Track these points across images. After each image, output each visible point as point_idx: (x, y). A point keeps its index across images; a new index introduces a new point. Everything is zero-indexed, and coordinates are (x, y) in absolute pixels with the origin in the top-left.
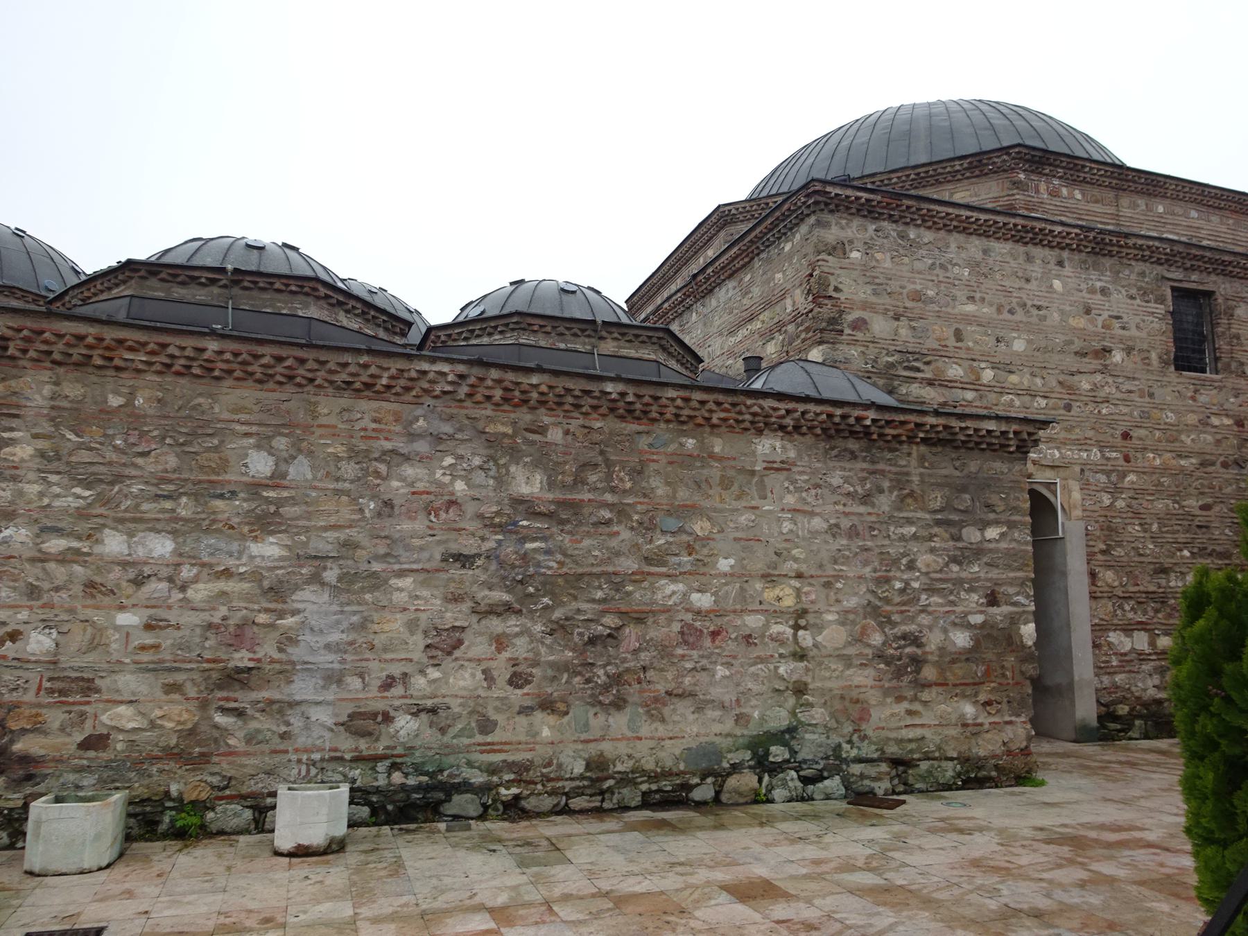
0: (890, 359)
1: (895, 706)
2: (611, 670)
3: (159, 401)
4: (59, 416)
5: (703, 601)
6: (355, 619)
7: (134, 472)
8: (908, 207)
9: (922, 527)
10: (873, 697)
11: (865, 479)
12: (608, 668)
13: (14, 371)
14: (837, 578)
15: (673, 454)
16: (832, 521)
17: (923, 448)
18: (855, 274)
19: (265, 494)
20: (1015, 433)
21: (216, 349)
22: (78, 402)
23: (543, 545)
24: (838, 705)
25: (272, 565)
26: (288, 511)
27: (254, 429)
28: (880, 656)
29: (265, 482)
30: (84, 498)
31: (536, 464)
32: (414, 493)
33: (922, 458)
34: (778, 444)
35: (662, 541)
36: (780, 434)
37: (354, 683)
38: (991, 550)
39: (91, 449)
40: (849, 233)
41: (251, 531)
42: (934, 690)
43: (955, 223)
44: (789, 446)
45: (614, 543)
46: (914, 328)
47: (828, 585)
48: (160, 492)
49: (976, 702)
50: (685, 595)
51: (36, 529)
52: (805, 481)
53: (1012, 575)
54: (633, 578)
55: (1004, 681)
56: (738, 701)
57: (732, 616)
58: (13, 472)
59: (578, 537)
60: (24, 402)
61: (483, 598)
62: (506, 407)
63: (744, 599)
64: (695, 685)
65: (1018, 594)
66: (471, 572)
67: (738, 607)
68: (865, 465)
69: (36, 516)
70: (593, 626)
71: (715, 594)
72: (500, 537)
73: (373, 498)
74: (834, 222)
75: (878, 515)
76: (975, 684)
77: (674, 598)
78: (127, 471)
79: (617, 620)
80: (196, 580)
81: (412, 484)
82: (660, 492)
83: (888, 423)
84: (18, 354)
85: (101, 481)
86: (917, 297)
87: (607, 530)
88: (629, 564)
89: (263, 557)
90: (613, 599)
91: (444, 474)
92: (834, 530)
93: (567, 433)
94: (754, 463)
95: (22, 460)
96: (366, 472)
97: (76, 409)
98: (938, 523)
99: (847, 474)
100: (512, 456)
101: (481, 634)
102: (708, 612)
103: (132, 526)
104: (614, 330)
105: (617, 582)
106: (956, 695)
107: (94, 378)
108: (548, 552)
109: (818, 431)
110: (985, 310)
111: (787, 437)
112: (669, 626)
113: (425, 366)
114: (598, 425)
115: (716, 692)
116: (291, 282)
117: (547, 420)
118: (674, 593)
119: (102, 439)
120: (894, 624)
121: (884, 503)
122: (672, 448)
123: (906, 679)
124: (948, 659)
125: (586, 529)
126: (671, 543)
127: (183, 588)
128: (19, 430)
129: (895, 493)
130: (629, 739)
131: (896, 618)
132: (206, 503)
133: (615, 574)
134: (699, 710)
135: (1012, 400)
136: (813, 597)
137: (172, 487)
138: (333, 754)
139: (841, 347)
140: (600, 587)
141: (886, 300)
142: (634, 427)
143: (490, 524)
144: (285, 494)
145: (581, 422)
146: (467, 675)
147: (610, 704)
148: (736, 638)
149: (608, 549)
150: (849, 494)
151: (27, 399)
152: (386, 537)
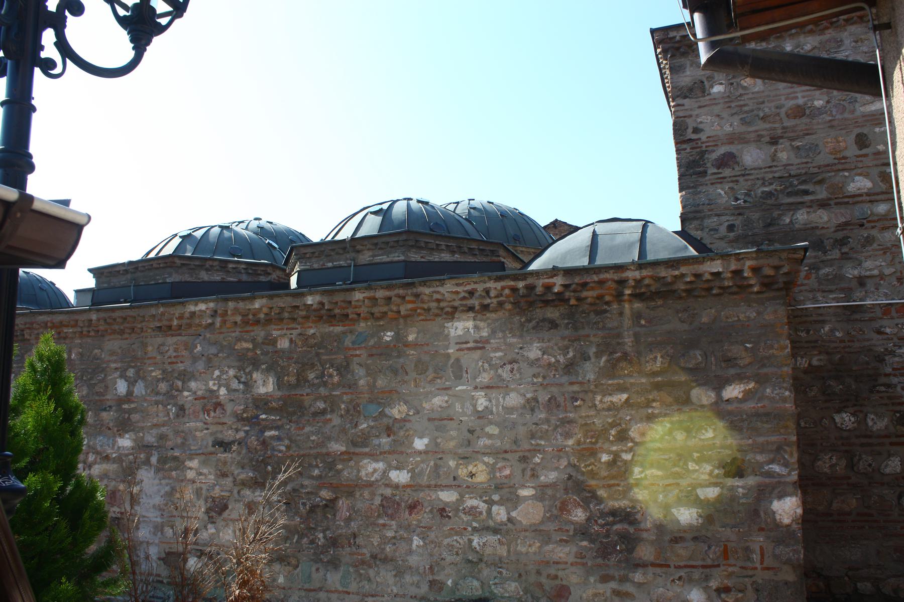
0: (766, 189)
1: (600, 586)
2: (329, 534)
3: (81, 354)
5: (400, 477)
6: (167, 489)
9: (638, 393)
10: (573, 577)
11: (567, 348)
12: (328, 532)
14: (536, 450)
15: (373, 347)
16: (529, 396)
17: (637, 305)
18: (717, 109)
19: (124, 406)
20: (755, 270)
23: (277, 433)
24: (532, 578)
25: (126, 452)
26: (135, 417)
27: (119, 365)
28: (582, 532)
31: (268, 370)
32: (196, 399)
33: (637, 316)
34: (470, 324)
35: (365, 426)
36: (471, 314)
37: (169, 532)
41: (118, 431)
42: (651, 570)
44: (482, 324)
45: (327, 430)
46: (798, 147)
47: (524, 459)
49: (706, 589)
50: (385, 473)
52: (500, 358)
53: (761, 439)
54: (342, 457)
55: (749, 564)
56: (431, 568)
57: (427, 492)
59: (301, 425)
61: (238, 475)
62: (248, 328)
63: (438, 476)
64: (395, 551)
65: (772, 462)
66: (230, 456)
67: (433, 483)
68: (567, 333)
70: (312, 497)
71: (412, 471)
72: (247, 428)
73: (175, 405)
74: (688, 63)
75: (581, 383)
76: (704, 567)
77: (375, 475)
79: (330, 494)
80: (95, 463)
81: (195, 393)
82: (362, 382)
83: (584, 285)
87: (322, 417)
88: (337, 447)
89: (123, 447)
90: (326, 475)
91: (214, 384)
92: (531, 405)
93: (291, 341)
94: (447, 347)
96: (172, 386)
98: (658, 387)
99: (545, 345)
100: (254, 364)
101: (239, 501)
102: (404, 487)
104: (366, 243)
105: (330, 462)
106: (680, 578)
108: (279, 438)
109: (508, 306)
111: (479, 316)
112: (372, 500)
113: (192, 308)
114: (312, 331)
115: (413, 560)
116: (160, 262)
117: (275, 333)
118: (375, 471)
120: (600, 501)
121: (589, 371)
122: (372, 343)
123: (613, 559)
124: (667, 538)
125: (307, 418)
126: (372, 427)
127: (90, 467)
129: (604, 359)
130: (339, 592)
131: (601, 493)
133: (328, 454)
134: (399, 573)
136: (507, 472)
138: (158, 578)
139: (703, 188)
140: (317, 466)
141: (761, 126)
142: (339, 329)
143: (240, 418)
144: (133, 406)
145: (299, 331)
146: (230, 532)
147: (328, 562)
148: (431, 511)
149: (322, 433)
150: (549, 364)
152: (183, 432)
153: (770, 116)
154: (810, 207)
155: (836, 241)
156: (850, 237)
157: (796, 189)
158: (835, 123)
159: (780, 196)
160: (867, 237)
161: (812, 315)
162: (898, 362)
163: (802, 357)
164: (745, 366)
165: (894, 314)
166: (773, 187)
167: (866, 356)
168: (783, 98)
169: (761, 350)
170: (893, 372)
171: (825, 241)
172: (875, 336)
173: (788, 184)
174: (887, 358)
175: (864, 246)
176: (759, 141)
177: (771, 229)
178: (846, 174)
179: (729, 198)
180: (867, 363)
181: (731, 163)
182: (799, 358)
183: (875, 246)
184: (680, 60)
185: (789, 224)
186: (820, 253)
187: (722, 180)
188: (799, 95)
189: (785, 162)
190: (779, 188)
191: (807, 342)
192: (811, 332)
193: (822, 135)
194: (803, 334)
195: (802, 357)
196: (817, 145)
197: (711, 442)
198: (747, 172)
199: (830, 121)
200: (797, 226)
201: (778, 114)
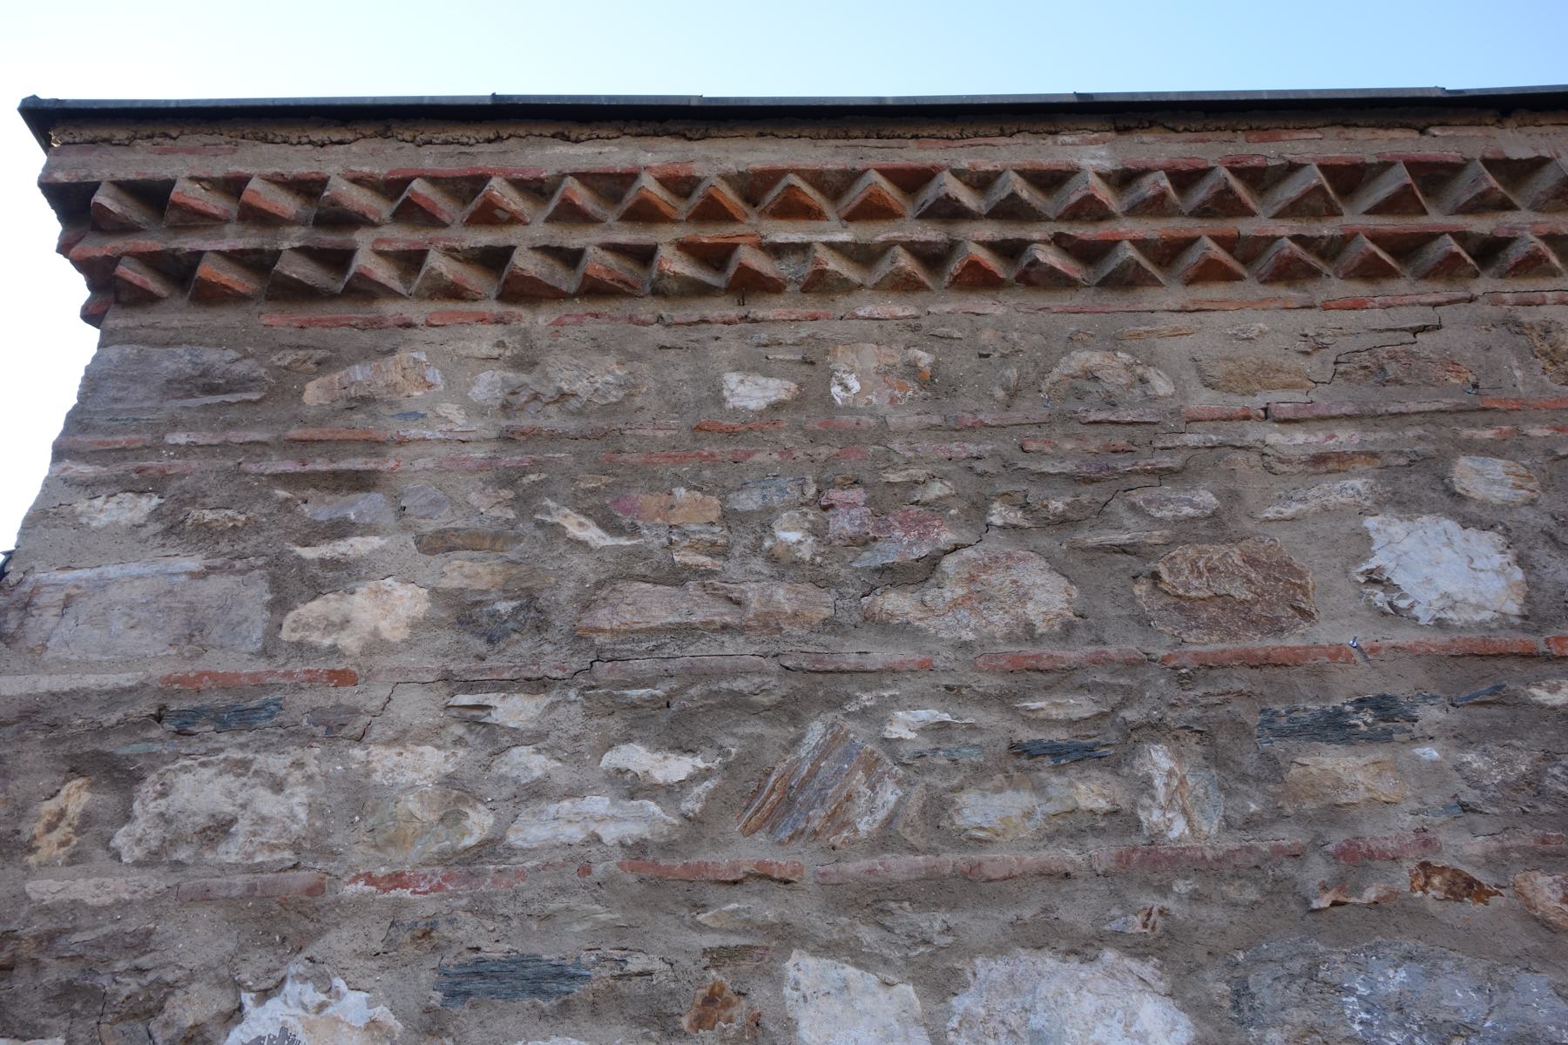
4: (537, 465)
7: (880, 655)
13: (366, 339)
21: (1108, 165)
22: (610, 410)
27: (1346, 438)
29: (1517, 640)
30: (670, 792)
39: (676, 577)
48: (1025, 735)
51: (424, 983)
58: (327, 697)
60: (393, 427)
69: (428, 906)
78: (849, 653)
84: (383, 273)
85: (739, 704)
95: (376, 645)
97: (600, 436)
103: (932, 922)
107: (660, 334)
119: (719, 534)
128: (370, 530)
132: (1274, 768)
137: (1081, 706)
151: (407, 416)
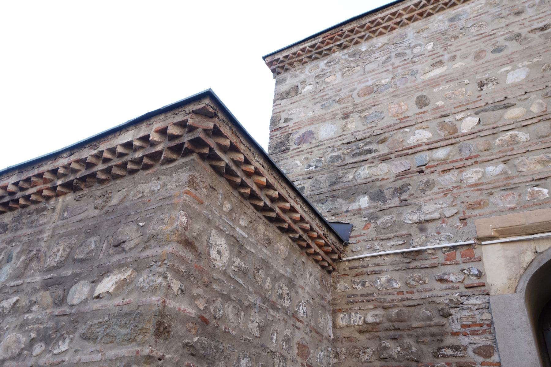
0: (335, 154)
8: (352, 31)
38: (94, 313)
40: (302, 76)
43: (406, 16)
46: (365, 117)
53: (111, 353)
74: (289, 77)
86: (369, 91)
110: (458, 64)
135: (513, 137)
153: (344, 98)
154: (373, 162)
155: (396, 189)
156: (409, 185)
157: (361, 150)
158: (398, 93)
159: (347, 158)
160: (427, 182)
161: (368, 266)
162: (467, 317)
163: (356, 313)
164: (131, 249)
165: (458, 258)
166: (341, 151)
167: (427, 309)
168: (356, 83)
169: (151, 228)
170: (462, 330)
171: (385, 191)
172: (439, 285)
173: (354, 147)
174: (453, 311)
175: (423, 191)
176: (334, 118)
177: (336, 187)
178: (407, 130)
179: (304, 166)
180: (429, 318)
181: (309, 139)
182: (353, 314)
183: (435, 189)
184: (283, 75)
185: (352, 181)
186: (380, 202)
187: (300, 153)
188: (369, 79)
189: (353, 130)
190: (345, 151)
191: (362, 295)
192: (367, 284)
193: (386, 104)
194: (359, 287)
195: (356, 313)
196: (382, 112)
197: (59, 359)
198: (321, 143)
199: (394, 91)
200: (359, 181)
201: (351, 96)
